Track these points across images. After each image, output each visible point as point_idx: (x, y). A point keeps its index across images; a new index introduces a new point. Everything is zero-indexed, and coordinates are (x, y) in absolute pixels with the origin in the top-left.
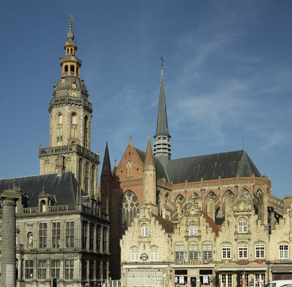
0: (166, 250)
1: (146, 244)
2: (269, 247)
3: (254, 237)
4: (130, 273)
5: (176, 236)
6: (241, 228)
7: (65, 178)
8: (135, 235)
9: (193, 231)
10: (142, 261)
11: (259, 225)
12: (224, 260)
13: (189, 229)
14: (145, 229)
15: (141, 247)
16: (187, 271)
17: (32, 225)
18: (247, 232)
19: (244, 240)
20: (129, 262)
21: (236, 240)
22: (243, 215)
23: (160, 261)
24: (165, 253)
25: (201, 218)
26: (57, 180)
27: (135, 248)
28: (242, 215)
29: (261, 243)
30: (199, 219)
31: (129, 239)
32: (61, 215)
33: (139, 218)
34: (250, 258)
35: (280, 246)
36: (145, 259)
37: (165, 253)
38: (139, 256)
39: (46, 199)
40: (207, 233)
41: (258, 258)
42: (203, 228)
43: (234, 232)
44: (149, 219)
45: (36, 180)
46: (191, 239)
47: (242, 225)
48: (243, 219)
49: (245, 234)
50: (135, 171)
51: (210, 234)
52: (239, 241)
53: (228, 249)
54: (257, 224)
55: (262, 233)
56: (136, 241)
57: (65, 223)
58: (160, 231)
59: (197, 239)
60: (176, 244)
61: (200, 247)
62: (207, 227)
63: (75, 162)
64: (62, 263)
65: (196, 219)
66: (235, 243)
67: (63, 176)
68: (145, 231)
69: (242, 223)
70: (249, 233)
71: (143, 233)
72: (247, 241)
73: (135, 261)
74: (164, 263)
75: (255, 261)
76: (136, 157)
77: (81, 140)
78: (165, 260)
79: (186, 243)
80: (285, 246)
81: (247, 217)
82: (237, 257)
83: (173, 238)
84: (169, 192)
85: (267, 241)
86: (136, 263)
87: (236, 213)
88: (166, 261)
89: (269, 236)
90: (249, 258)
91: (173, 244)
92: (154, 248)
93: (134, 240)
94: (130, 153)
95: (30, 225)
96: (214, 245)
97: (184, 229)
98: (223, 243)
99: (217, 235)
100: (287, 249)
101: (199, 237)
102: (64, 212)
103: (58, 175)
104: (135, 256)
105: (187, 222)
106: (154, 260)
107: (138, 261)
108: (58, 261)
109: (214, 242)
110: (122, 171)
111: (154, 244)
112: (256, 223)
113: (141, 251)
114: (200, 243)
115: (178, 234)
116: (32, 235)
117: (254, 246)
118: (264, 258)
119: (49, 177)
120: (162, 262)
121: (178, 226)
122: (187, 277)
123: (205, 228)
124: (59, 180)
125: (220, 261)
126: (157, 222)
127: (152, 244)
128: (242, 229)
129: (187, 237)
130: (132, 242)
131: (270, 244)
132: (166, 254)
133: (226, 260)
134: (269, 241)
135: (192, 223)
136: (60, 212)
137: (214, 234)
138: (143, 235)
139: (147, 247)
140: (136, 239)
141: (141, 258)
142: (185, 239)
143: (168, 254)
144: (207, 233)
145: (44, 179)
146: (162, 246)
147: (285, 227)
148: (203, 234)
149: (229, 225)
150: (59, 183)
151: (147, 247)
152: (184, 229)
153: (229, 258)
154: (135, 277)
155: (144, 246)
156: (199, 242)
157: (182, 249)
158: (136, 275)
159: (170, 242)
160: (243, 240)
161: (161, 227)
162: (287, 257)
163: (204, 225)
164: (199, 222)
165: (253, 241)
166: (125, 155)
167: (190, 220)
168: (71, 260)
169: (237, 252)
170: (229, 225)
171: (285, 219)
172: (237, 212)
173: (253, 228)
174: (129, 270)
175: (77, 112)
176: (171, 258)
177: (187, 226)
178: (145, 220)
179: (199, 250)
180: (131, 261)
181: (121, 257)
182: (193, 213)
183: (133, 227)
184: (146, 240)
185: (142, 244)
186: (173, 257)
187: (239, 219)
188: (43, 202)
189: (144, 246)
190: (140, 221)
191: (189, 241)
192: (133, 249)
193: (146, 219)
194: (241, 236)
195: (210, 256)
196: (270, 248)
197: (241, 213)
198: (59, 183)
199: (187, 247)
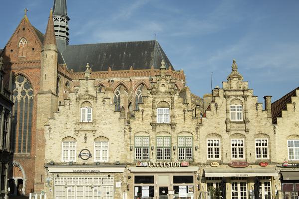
1: (89, 135)
2: (275, 143)
3: (253, 127)
4: (59, 181)
5: (137, 122)
6: (233, 114)
8: (70, 119)
9: (163, 116)
10: (81, 161)
13: (157, 112)
14: (86, 111)
15: (81, 138)
16: (153, 176)
18: (242, 120)
19: (240, 132)
20: (58, 162)
21: (228, 131)
22: (238, 96)
23: (111, 162)
27: (69, 140)
28: (235, 96)
29: (262, 136)
30: (172, 99)
33: (79, 93)
36: (86, 158)
37: (118, 148)
38: (77, 153)
42: (178, 112)
44: (95, 95)
46: (161, 129)
47: (234, 110)
48: (236, 101)
49: (240, 123)
51: (189, 121)
52: (232, 133)
53: (215, 145)
54: (257, 109)
55: (264, 123)
56: (72, 129)
58: (112, 115)
59: (169, 129)
60: (137, 135)
61: (174, 140)
62: (184, 111)
65: (167, 99)
66: (226, 136)
68: (86, 114)
69: (234, 107)
70: (245, 122)
71: (84, 117)
72: (243, 133)
73: (69, 160)
74: (117, 164)
75: (256, 163)
78: (119, 160)
79: (153, 134)
81: (242, 99)
82: (230, 156)
83: (132, 125)
85: (271, 134)
86: (71, 165)
87: (227, 93)
88: (122, 161)
89: (274, 128)
91: (132, 134)
92: (101, 141)
93: (68, 126)
96: (196, 138)
97: (151, 113)
104: (69, 152)
105: (154, 102)
106: (101, 160)
107: (74, 161)
109: (195, 133)
111: (101, 134)
112: (255, 108)
113: (80, 144)
114: (176, 135)
115: (140, 120)
117: (253, 140)
120: (114, 164)
122: (154, 186)
125: (205, 162)
127: (98, 134)
128: (234, 115)
129: (154, 125)
130: (65, 130)
131: (276, 138)
132: (120, 150)
133: (214, 161)
134: (275, 134)
135: (161, 105)
138: (84, 119)
139: (91, 139)
140: (71, 125)
141: (80, 156)
142: (151, 127)
143: (124, 152)
146: (115, 137)
147: (294, 114)
148: (179, 121)
149: (217, 109)
151: (91, 139)
152: (150, 113)
153: (217, 159)
154: (68, 188)
155: (85, 138)
156: (173, 133)
157: (145, 143)
158: (70, 184)
159: (127, 131)
160: (237, 132)
163: (180, 108)
164: (173, 103)
165: (251, 133)
167: (158, 100)
169: (230, 148)
170: (217, 109)
171: (294, 103)
172: (230, 91)
173: (251, 114)
174: (58, 176)
176: (128, 157)
177: (154, 107)
178: (87, 96)
179: (173, 145)
180: (63, 161)
183: (67, 107)
184: (88, 127)
185: (82, 134)
186: (132, 155)
187: (231, 101)
189: (85, 138)
190: (79, 98)
192: (66, 141)
193: (89, 95)
194: (234, 125)
195: (190, 154)
196: (276, 144)
197: (234, 93)
199: (155, 140)
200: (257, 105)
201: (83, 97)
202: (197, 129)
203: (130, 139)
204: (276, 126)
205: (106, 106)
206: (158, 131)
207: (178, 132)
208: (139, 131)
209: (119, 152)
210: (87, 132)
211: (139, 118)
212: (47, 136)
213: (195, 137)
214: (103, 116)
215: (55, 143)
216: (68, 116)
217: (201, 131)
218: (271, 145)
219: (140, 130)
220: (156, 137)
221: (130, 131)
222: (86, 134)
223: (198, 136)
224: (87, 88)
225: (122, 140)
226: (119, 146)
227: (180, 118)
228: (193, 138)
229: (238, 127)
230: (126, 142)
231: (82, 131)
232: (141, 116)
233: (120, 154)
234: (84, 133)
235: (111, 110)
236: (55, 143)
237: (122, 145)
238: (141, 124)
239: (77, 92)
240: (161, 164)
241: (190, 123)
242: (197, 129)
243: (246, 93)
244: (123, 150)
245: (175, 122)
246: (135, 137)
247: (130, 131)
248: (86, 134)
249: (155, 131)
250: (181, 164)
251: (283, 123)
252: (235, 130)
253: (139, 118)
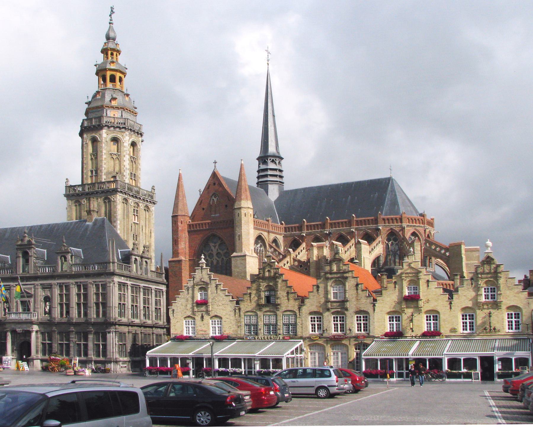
0: (232, 321)
2: (374, 319)
3: (351, 306)
5: (246, 303)
11: (359, 291)
24: (230, 325)
31: (181, 307)
33: (195, 280)
37: (230, 325)
51: (292, 302)
54: (357, 289)
55: (363, 300)
57: (94, 286)
61: (280, 318)
62: (288, 293)
85: (370, 310)
87: (329, 276)
91: (242, 313)
98: (311, 313)
109: (297, 312)
111: (216, 314)
112: (355, 288)
115: (249, 301)
123: (285, 294)
125: (308, 335)
127: (212, 314)
131: (375, 314)
134: (374, 310)
140: (189, 306)
143: (234, 327)
144: (288, 299)
146: (227, 316)
151: (206, 317)
155: (202, 317)
159: (237, 311)
173: (351, 294)
176: (239, 332)
181: (171, 331)
182: (267, 274)
189: (202, 317)
196: (376, 320)
201: (199, 283)
202: (299, 308)
203: (240, 317)
205: (219, 291)
207: (283, 311)
208: (248, 310)
209: (231, 328)
210: (204, 313)
211: (247, 300)
213: (298, 314)
214: (216, 298)
215: (178, 322)
216: (187, 300)
217: (303, 311)
218: (370, 321)
219: (249, 310)
220: (264, 315)
221: (240, 311)
222: (202, 314)
223: (301, 314)
224: (202, 275)
225: (233, 318)
226: (231, 323)
227: (284, 299)
228: (296, 316)
230: (236, 319)
231: (199, 312)
232: (249, 298)
233: (232, 329)
234: (202, 313)
235: (223, 293)
236: (178, 322)
237: (234, 322)
238: (250, 304)
239: (194, 279)
240: (266, 338)
241: (294, 303)
242: (299, 308)
243: (345, 275)
244: (234, 326)
245: (279, 302)
246: (244, 316)
247: (240, 311)
248: (202, 314)
249: (261, 311)
250: (283, 338)
251: (383, 300)
252: (336, 308)
253: (247, 300)
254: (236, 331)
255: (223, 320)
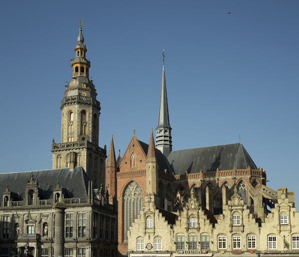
7: (76, 174)
10: (147, 250)
12: (220, 250)
17: (47, 216)
23: (164, 250)
25: (200, 211)
26: (70, 174)
32: (74, 207)
34: (243, 248)
35: (269, 238)
36: (150, 248)
37: (167, 243)
38: (145, 246)
39: (60, 192)
40: (205, 225)
41: (250, 248)
42: (201, 221)
43: (228, 225)
44: (154, 211)
45: (50, 175)
50: (139, 163)
51: (207, 226)
52: (233, 233)
55: (253, 226)
62: (205, 220)
63: (85, 157)
64: (75, 251)
65: (195, 213)
67: (75, 171)
73: (140, 250)
75: (247, 251)
76: (139, 149)
77: (90, 136)
79: (186, 234)
80: (273, 238)
83: (174, 229)
84: (171, 183)
88: (169, 250)
89: (260, 229)
90: (242, 249)
91: (175, 235)
94: (133, 146)
95: (46, 216)
98: (218, 235)
99: (214, 227)
100: (275, 240)
101: (199, 229)
102: (76, 204)
103: (70, 170)
106: (158, 250)
108: (71, 249)
110: (126, 163)
111: (157, 235)
113: (146, 240)
114: (199, 234)
115: (179, 226)
116: (47, 226)
118: (255, 248)
119: (61, 172)
120: (165, 252)
121: (179, 219)
124: (71, 174)
126: (161, 215)
127: (156, 235)
136: (73, 204)
137: (211, 226)
139: (152, 237)
141: (146, 247)
142: (185, 230)
144: (205, 225)
145: (57, 174)
146: (165, 236)
148: (202, 226)
150: (71, 177)
151: (152, 237)
153: (224, 249)
155: (149, 237)
159: (172, 233)
161: (164, 219)
162: (275, 248)
163: (202, 218)
166: (129, 147)
168: (83, 249)
175: (87, 110)
183: (139, 219)
188: (58, 195)
189: (149, 237)
191: (189, 232)
192: (138, 239)
195: (208, 246)
198: (71, 177)
200: (249, 215)
203: (174, 237)
204: (261, 228)
205: (160, 218)
206: (189, 232)
212: (129, 236)
229: (237, 229)
254: (171, 247)
255: (163, 239)
